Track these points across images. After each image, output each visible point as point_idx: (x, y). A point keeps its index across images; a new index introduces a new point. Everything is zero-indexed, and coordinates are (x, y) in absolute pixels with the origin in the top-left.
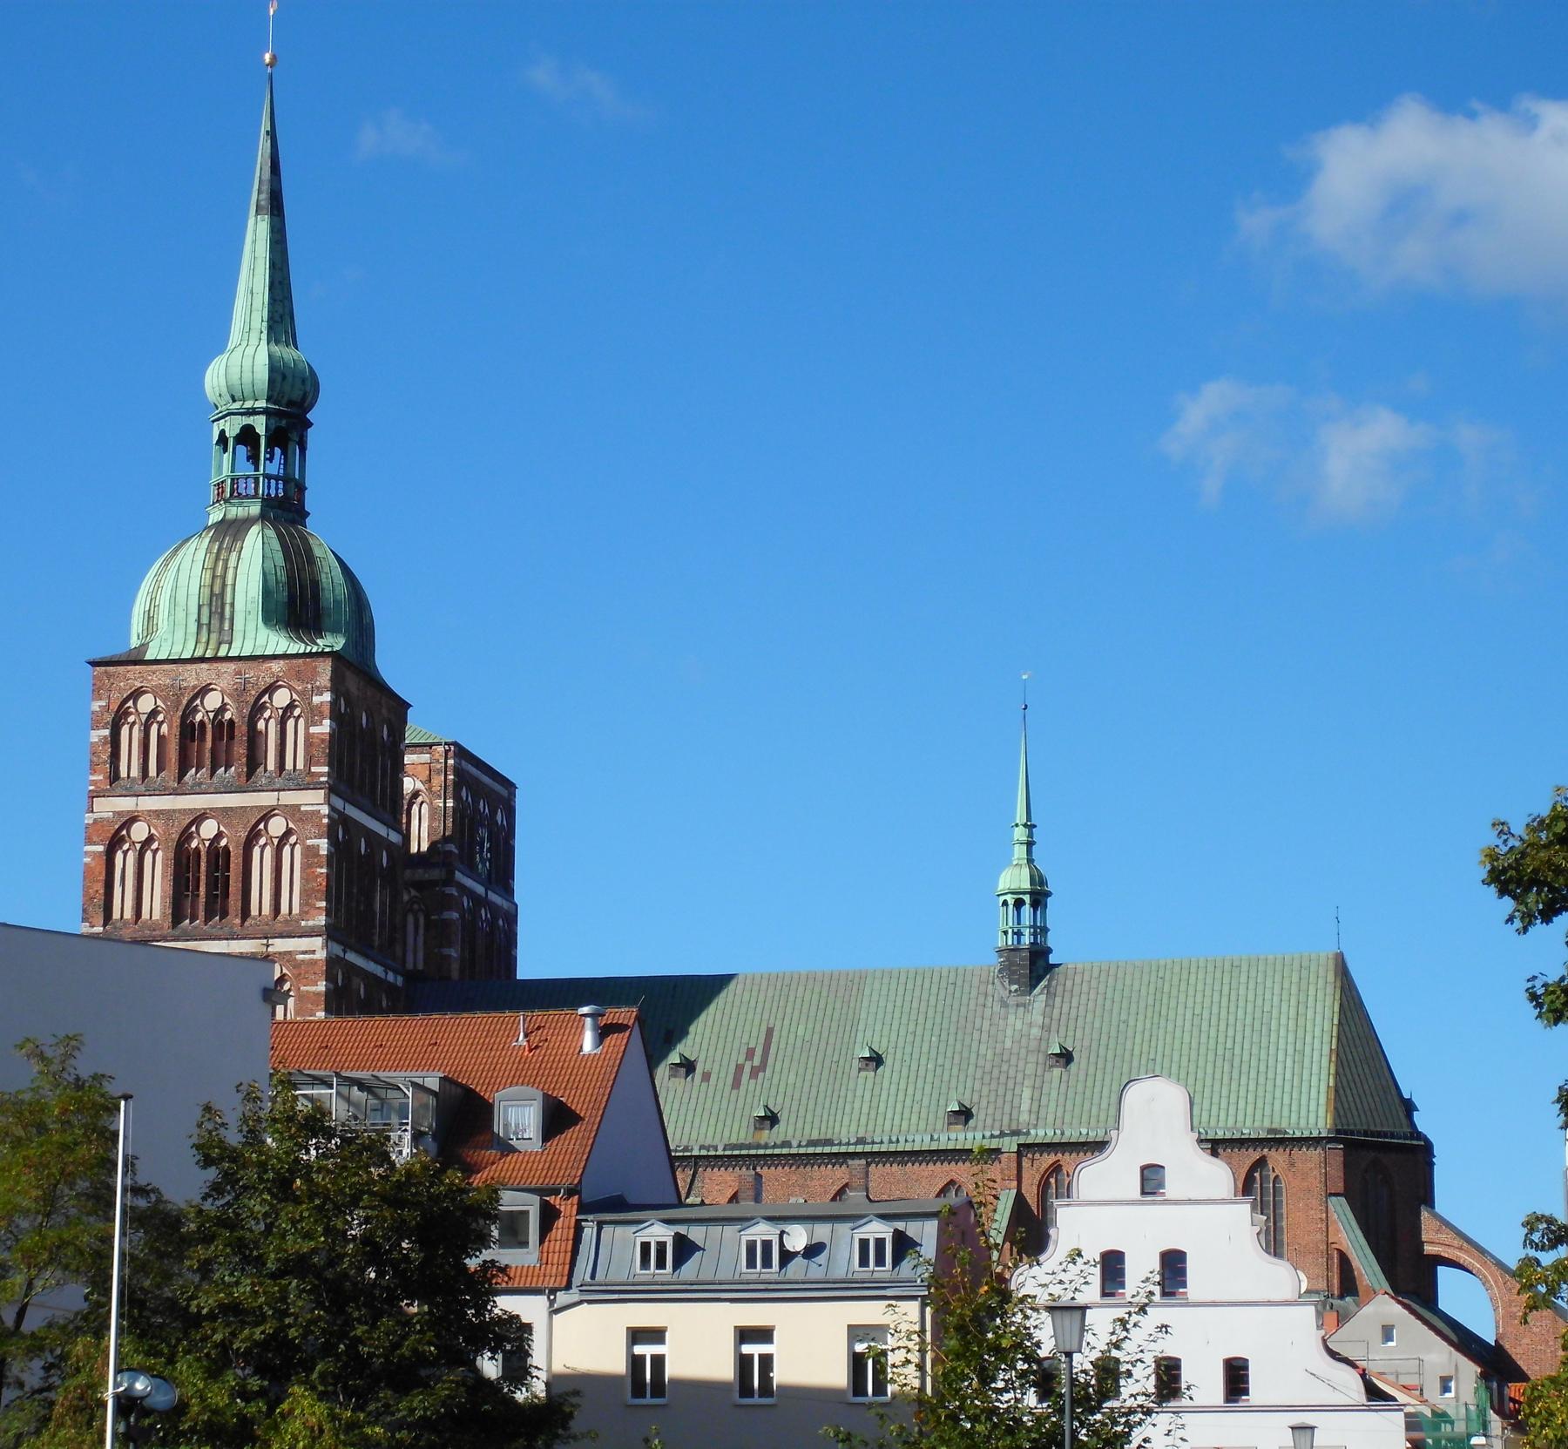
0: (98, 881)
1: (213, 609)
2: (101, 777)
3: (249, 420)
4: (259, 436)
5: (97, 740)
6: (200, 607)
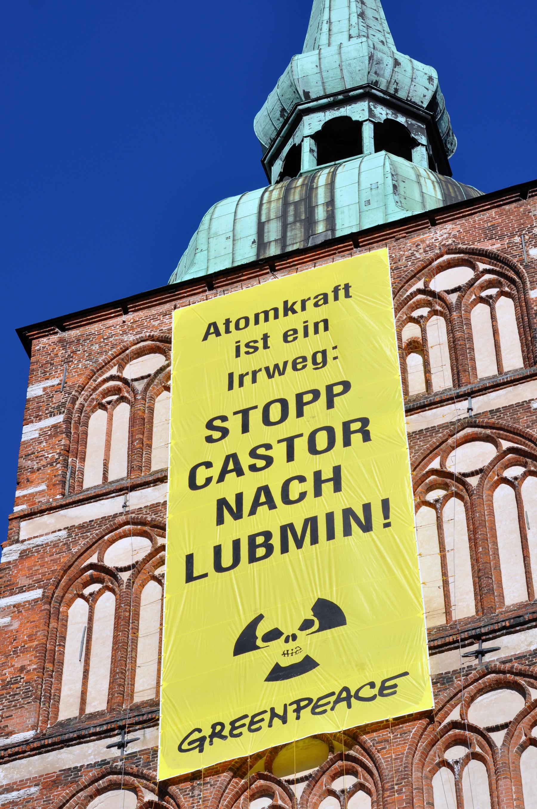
0: (25, 650)
1: (290, 219)
2: (43, 487)
3: (342, 112)
4: (359, 124)
5: (37, 436)
6: (261, 227)
